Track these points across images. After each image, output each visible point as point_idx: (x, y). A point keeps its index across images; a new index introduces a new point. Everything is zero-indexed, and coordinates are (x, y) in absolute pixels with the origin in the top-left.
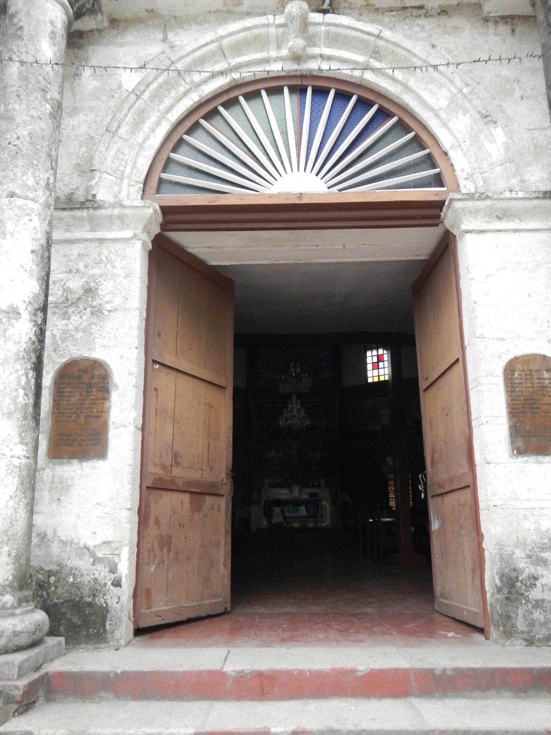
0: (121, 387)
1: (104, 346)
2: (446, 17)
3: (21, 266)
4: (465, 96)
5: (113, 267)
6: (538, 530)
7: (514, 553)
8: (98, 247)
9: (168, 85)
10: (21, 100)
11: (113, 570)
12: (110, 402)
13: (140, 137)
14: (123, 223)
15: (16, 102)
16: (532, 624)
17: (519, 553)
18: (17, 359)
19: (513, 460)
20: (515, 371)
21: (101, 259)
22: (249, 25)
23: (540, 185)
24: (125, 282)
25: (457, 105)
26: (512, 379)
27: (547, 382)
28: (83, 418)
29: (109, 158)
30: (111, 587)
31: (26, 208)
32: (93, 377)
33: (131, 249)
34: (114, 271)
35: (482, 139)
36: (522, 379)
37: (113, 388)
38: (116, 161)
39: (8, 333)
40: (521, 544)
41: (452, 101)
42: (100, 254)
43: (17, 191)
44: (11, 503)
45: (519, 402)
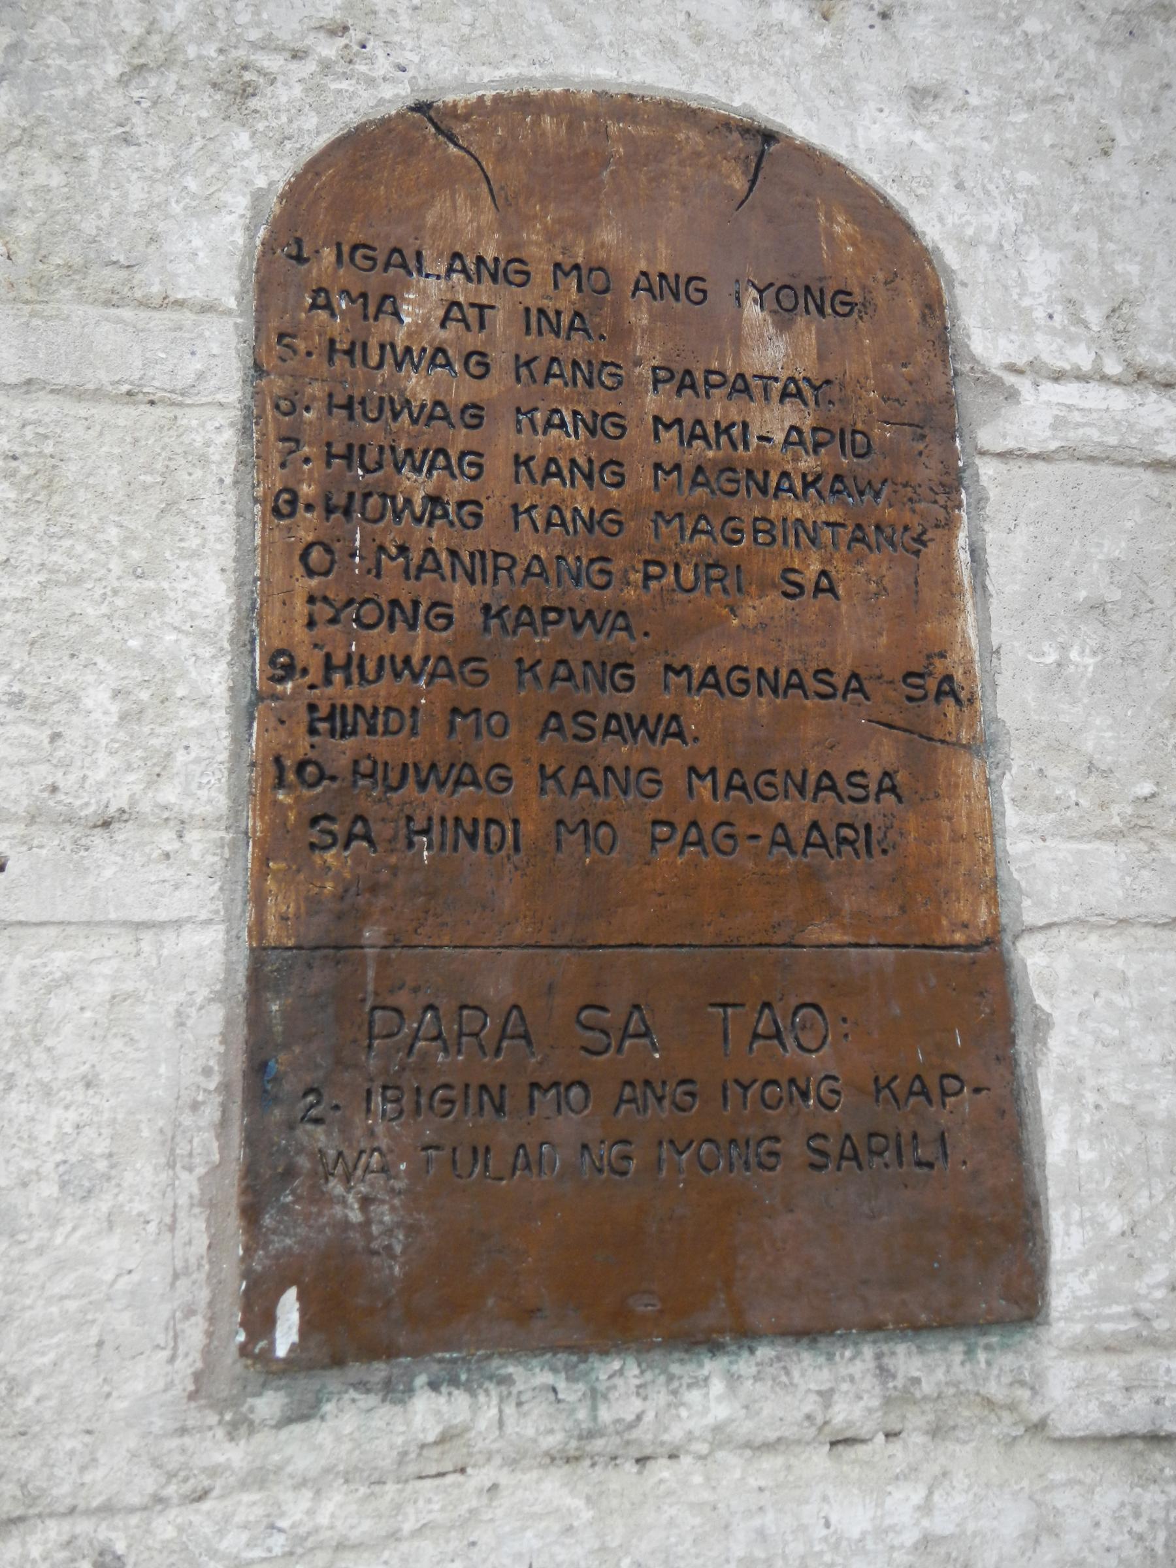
19: (235, 1455)
20: (405, 261)
26: (355, 351)
27: (774, 420)
36: (479, 363)
45: (419, 642)
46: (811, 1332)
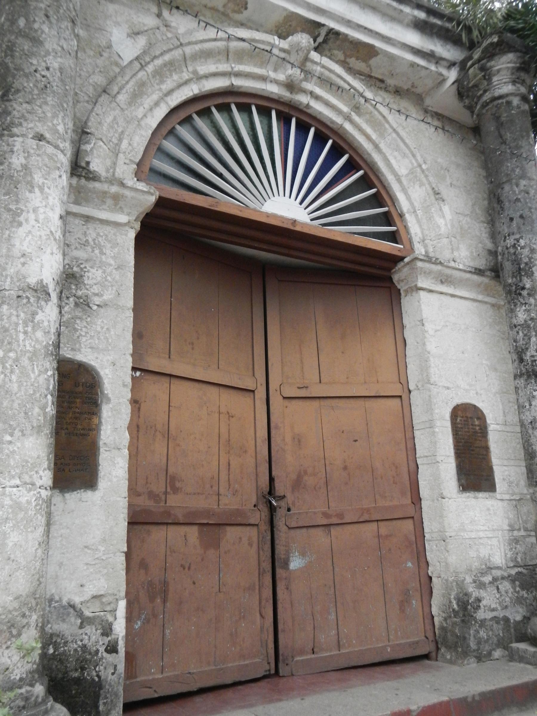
0: (114, 400)
1: (91, 348)
2: (399, 97)
3: (51, 232)
4: (423, 171)
5: (102, 253)
6: (478, 557)
7: (465, 579)
8: (83, 225)
9: (171, 66)
10: (50, 22)
11: (107, 631)
12: (100, 418)
13: (140, 113)
14: (116, 205)
15: (44, 22)
16: (479, 643)
17: (469, 579)
18: (46, 355)
21: (87, 241)
22: (257, 38)
23: (466, 261)
24: (116, 275)
25: (416, 177)
27: (477, 428)
28: (63, 435)
29: (106, 125)
30: (105, 654)
31: (56, 159)
32: (77, 385)
33: (124, 237)
34: (103, 257)
35: (432, 211)
37: (104, 401)
38: (111, 130)
39: (38, 318)
40: (469, 570)
41: (412, 172)
42: (85, 234)
43: (47, 135)
44: (40, 551)
46: (485, 491)
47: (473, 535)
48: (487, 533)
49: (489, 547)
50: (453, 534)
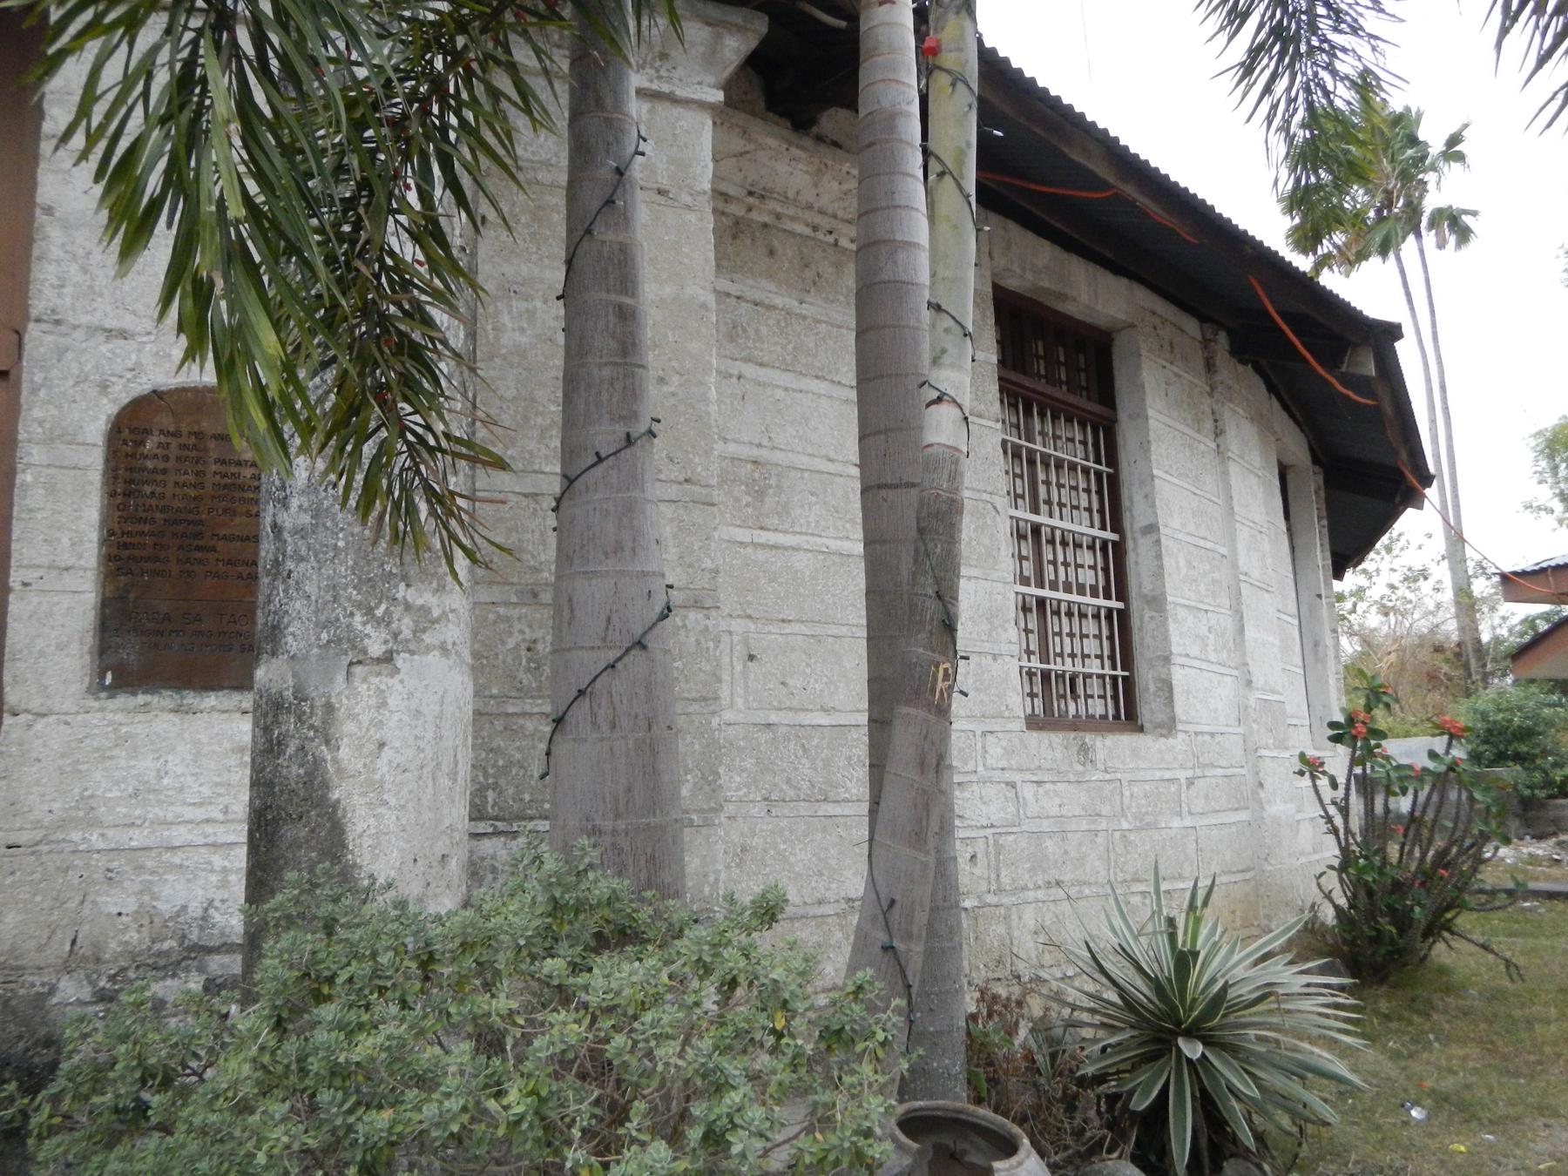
6: (146, 915)
7: (53, 990)
17: (71, 990)
19: (97, 704)
20: (148, 432)
26: (133, 456)
36: (166, 458)
45: (146, 528)
47: (117, 837)
48: (209, 829)
49: (214, 878)
50: (24, 837)
